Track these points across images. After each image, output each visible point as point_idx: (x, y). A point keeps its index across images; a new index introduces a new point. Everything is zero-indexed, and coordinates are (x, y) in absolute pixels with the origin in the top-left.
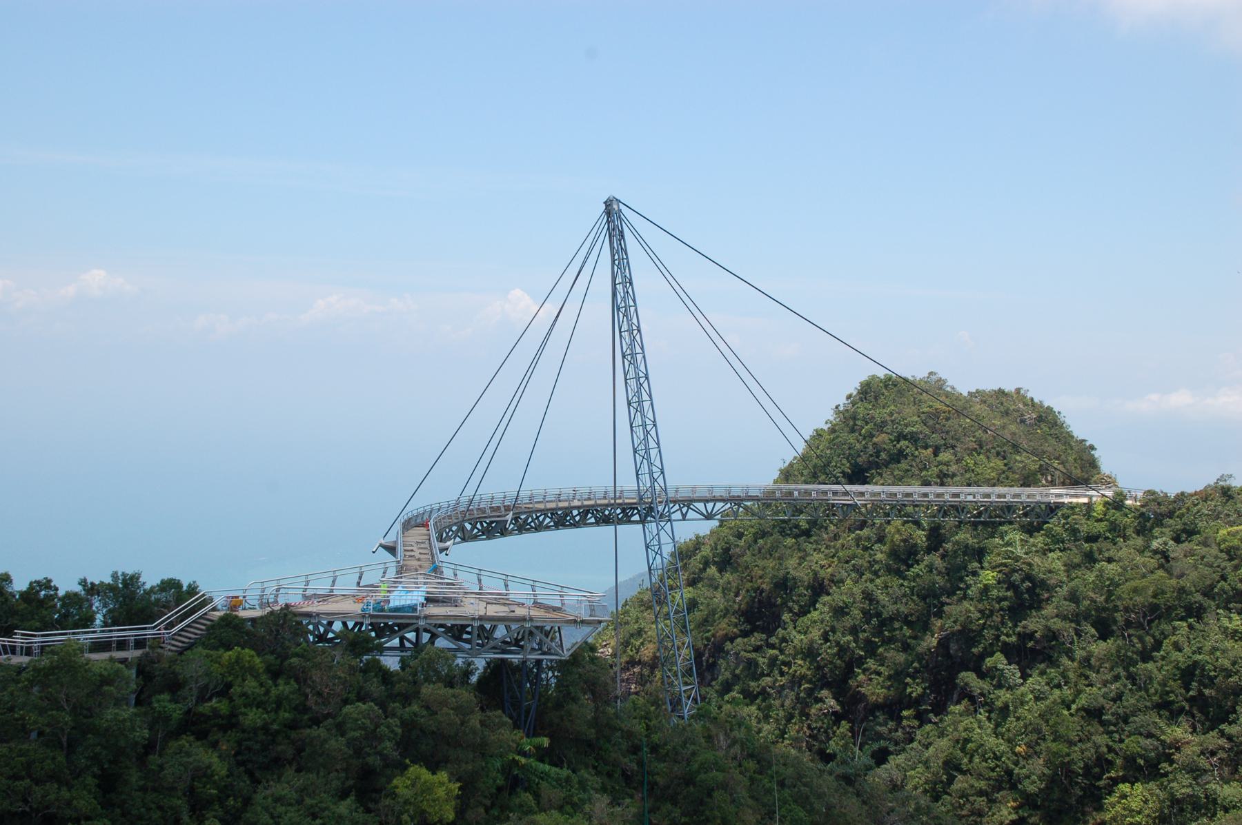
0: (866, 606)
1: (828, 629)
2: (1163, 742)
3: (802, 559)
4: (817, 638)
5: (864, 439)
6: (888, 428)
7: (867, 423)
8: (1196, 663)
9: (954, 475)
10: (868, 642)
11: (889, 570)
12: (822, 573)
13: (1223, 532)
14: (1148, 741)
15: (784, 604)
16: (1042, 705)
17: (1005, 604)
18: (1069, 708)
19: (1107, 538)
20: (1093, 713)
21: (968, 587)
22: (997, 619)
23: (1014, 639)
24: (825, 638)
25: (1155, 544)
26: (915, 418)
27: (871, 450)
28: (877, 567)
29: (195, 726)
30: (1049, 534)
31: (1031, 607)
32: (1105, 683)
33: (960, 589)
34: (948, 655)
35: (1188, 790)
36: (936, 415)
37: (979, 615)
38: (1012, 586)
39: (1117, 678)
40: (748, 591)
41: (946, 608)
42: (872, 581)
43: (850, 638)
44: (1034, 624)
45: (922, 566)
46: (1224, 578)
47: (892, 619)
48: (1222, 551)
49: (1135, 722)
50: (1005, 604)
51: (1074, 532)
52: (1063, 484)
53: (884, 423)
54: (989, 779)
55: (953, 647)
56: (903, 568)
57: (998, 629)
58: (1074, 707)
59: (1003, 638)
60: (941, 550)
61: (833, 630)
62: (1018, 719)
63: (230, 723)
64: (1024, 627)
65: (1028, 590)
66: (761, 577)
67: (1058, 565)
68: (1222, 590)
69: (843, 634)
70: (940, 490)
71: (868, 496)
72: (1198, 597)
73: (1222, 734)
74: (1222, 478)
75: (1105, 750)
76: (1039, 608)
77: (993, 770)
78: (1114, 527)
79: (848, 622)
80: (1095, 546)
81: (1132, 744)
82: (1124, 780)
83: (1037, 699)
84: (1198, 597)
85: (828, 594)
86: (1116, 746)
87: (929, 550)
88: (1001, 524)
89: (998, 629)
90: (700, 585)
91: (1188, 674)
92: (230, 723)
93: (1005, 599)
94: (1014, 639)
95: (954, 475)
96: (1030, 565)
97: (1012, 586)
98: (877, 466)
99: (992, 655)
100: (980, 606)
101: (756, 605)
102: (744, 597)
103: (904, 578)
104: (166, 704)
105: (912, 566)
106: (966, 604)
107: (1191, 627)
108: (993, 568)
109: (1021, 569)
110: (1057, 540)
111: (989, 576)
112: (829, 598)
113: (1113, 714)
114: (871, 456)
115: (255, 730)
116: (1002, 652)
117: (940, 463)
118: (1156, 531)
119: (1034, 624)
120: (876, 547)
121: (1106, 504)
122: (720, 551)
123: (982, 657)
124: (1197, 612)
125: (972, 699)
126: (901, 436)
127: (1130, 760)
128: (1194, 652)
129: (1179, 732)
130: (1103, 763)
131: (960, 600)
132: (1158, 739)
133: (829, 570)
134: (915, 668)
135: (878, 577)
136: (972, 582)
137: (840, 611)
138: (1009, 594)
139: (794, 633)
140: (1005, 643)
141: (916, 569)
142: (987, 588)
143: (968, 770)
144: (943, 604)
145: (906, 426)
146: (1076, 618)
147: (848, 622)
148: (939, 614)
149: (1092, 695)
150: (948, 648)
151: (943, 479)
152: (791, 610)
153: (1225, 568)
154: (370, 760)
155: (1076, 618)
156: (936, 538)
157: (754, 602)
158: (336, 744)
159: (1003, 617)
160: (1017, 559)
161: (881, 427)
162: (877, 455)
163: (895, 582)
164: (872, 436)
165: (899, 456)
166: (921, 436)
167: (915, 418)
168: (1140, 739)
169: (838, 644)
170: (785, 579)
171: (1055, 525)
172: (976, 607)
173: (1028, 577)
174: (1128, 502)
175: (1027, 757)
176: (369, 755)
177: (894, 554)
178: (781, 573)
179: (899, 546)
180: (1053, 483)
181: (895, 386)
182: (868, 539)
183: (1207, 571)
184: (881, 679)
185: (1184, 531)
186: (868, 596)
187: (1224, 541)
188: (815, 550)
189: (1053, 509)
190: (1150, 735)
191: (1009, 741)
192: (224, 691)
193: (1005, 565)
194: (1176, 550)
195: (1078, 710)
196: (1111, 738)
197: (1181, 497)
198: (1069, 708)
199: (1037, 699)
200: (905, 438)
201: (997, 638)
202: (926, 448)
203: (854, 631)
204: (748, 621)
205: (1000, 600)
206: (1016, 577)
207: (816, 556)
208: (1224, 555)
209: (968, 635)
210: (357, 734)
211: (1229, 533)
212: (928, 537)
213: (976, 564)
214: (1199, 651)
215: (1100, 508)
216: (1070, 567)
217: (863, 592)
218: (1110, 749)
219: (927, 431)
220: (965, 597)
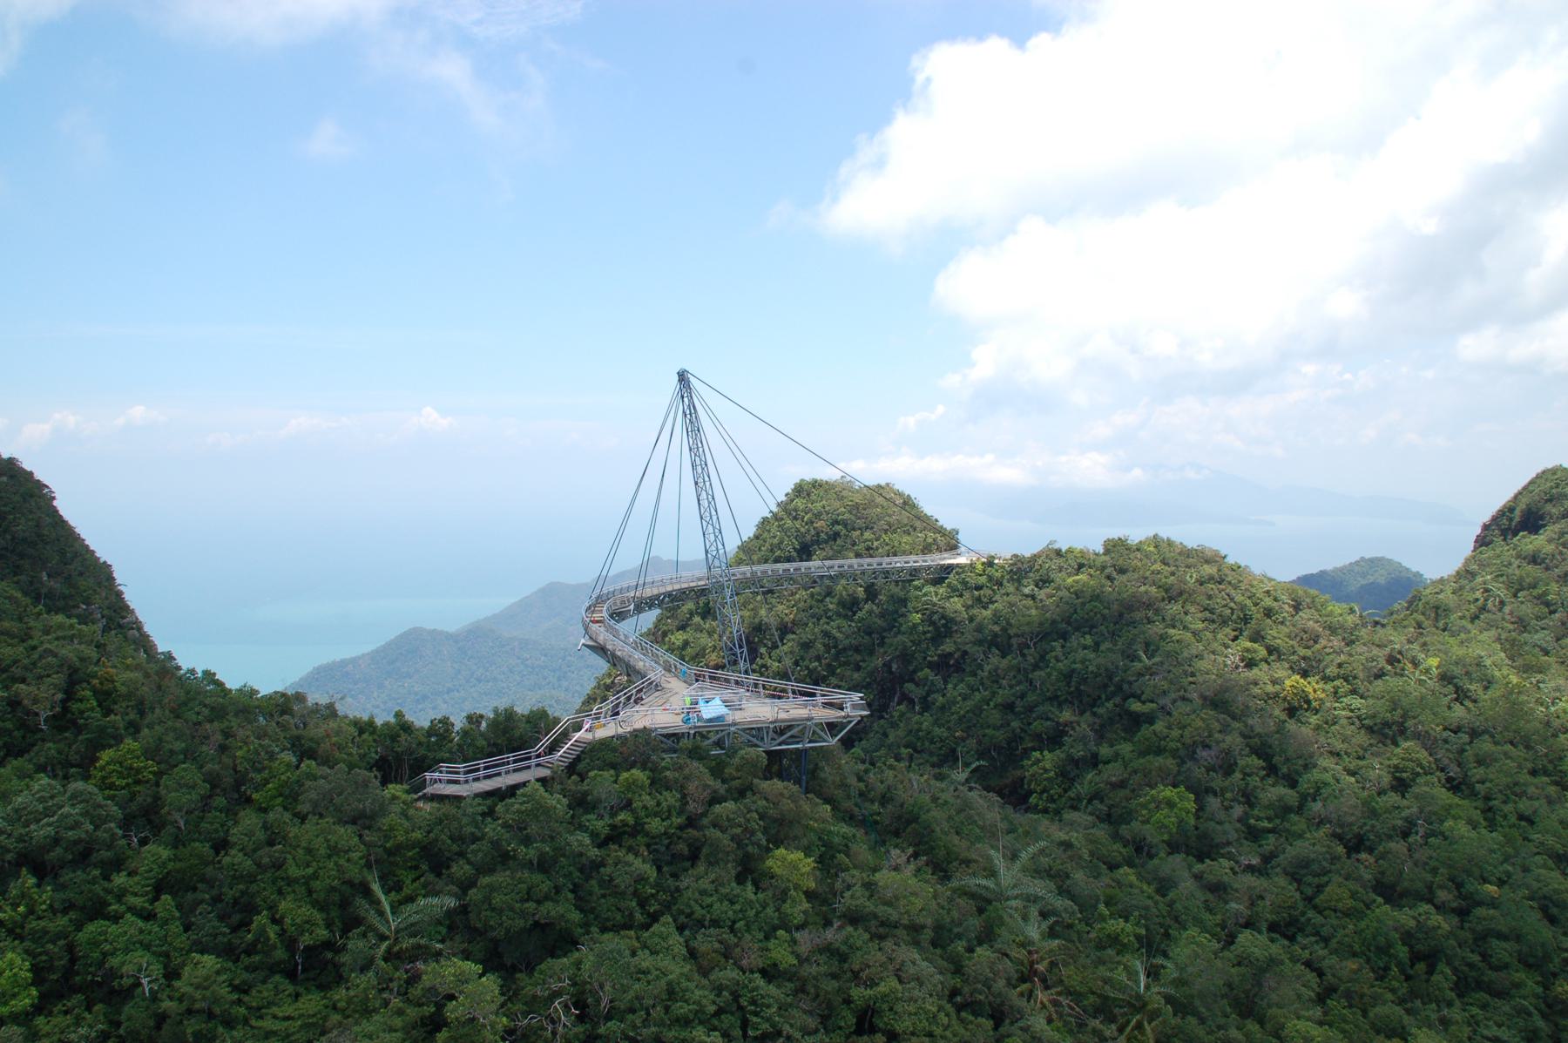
0: (826, 641)
2: (1058, 723)
3: (771, 609)
5: (807, 524)
6: (824, 516)
7: (806, 514)
8: (1073, 671)
9: (877, 549)
10: (829, 665)
11: (839, 615)
12: (786, 619)
13: (1070, 580)
14: (1049, 723)
15: (761, 641)
16: (969, 703)
17: (929, 635)
18: (988, 705)
20: (1009, 707)
22: (924, 646)
23: (936, 658)
24: (796, 663)
25: (1027, 591)
26: (843, 510)
27: (813, 532)
28: (830, 614)
29: (615, 836)
30: (949, 586)
31: (945, 637)
32: (1011, 687)
33: (895, 627)
34: (891, 672)
35: (1082, 753)
36: (857, 506)
37: (911, 644)
38: (932, 623)
39: (1019, 683)
41: (886, 640)
42: (828, 624)
43: (817, 664)
44: (948, 646)
45: (864, 612)
46: (1076, 612)
47: (845, 649)
50: (929, 635)
51: (964, 583)
52: (946, 550)
53: (820, 513)
54: (939, 755)
55: (894, 667)
56: (850, 613)
57: (924, 653)
58: (992, 704)
59: (929, 658)
61: (802, 658)
62: (953, 714)
63: (637, 829)
64: (943, 650)
65: (943, 625)
67: (959, 607)
68: (1076, 620)
69: (810, 660)
70: (869, 560)
71: (836, 568)
73: (1094, 714)
74: (1051, 543)
75: (1019, 730)
76: (951, 637)
77: (940, 749)
78: (990, 578)
79: (813, 653)
80: (982, 592)
81: (1037, 726)
82: (1034, 749)
83: (964, 699)
85: (794, 633)
86: (1026, 728)
87: (866, 601)
88: (913, 580)
89: (924, 653)
90: (688, 629)
91: (1068, 676)
92: (637, 829)
93: (929, 632)
94: (936, 658)
95: (877, 549)
97: (932, 623)
98: (818, 542)
99: (922, 669)
100: (912, 638)
103: (852, 621)
104: (595, 823)
105: (856, 612)
106: (900, 637)
107: (1063, 647)
108: (917, 612)
110: (954, 590)
111: (917, 617)
112: (794, 636)
115: (659, 836)
116: (928, 667)
117: (866, 540)
118: (1025, 582)
119: (948, 646)
120: (828, 599)
121: (983, 564)
122: (701, 605)
123: (915, 672)
124: (1064, 636)
125: (912, 702)
126: (836, 522)
127: (1038, 737)
129: (1066, 715)
130: (1015, 739)
131: (895, 636)
133: (792, 616)
135: (833, 621)
137: (806, 646)
138: (930, 629)
139: (770, 661)
140: (929, 662)
141: (860, 614)
142: (915, 626)
143: (922, 751)
145: (838, 515)
146: (979, 642)
147: (813, 653)
148: (882, 644)
149: (1003, 695)
150: (890, 667)
151: (870, 551)
152: (765, 646)
154: (750, 849)
155: (979, 642)
156: (871, 592)
158: (725, 840)
159: (928, 644)
160: (935, 605)
161: (818, 516)
162: (818, 534)
163: (844, 623)
164: (812, 523)
165: (836, 536)
167: (843, 510)
168: (1042, 721)
169: (807, 668)
170: (760, 624)
171: (952, 579)
173: (943, 617)
174: (996, 561)
175: (963, 739)
176: (747, 845)
177: (842, 603)
178: (757, 620)
180: (939, 550)
182: (819, 594)
185: (1041, 580)
186: (826, 634)
187: (1072, 587)
189: (949, 569)
190: (1048, 719)
191: (949, 728)
192: (628, 805)
193: (926, 609)
194: (1041, 594)
195: (995, 707)
197: (1034, 558)
198: (988, 705)
199: (964, 699)
201: (925, 658)
202: (854, 529)
205: (925, 633)
206: (935, 617)
207: (781, 607)
208: (1073, 596)
209: (905, 657)
210: (738, 830)
212: (865, 591)
213: (904, 609)
214: (1074, 662)
215: (980, 567)
216: (968, 608)
219: (853, 518)
220: (899, 632)
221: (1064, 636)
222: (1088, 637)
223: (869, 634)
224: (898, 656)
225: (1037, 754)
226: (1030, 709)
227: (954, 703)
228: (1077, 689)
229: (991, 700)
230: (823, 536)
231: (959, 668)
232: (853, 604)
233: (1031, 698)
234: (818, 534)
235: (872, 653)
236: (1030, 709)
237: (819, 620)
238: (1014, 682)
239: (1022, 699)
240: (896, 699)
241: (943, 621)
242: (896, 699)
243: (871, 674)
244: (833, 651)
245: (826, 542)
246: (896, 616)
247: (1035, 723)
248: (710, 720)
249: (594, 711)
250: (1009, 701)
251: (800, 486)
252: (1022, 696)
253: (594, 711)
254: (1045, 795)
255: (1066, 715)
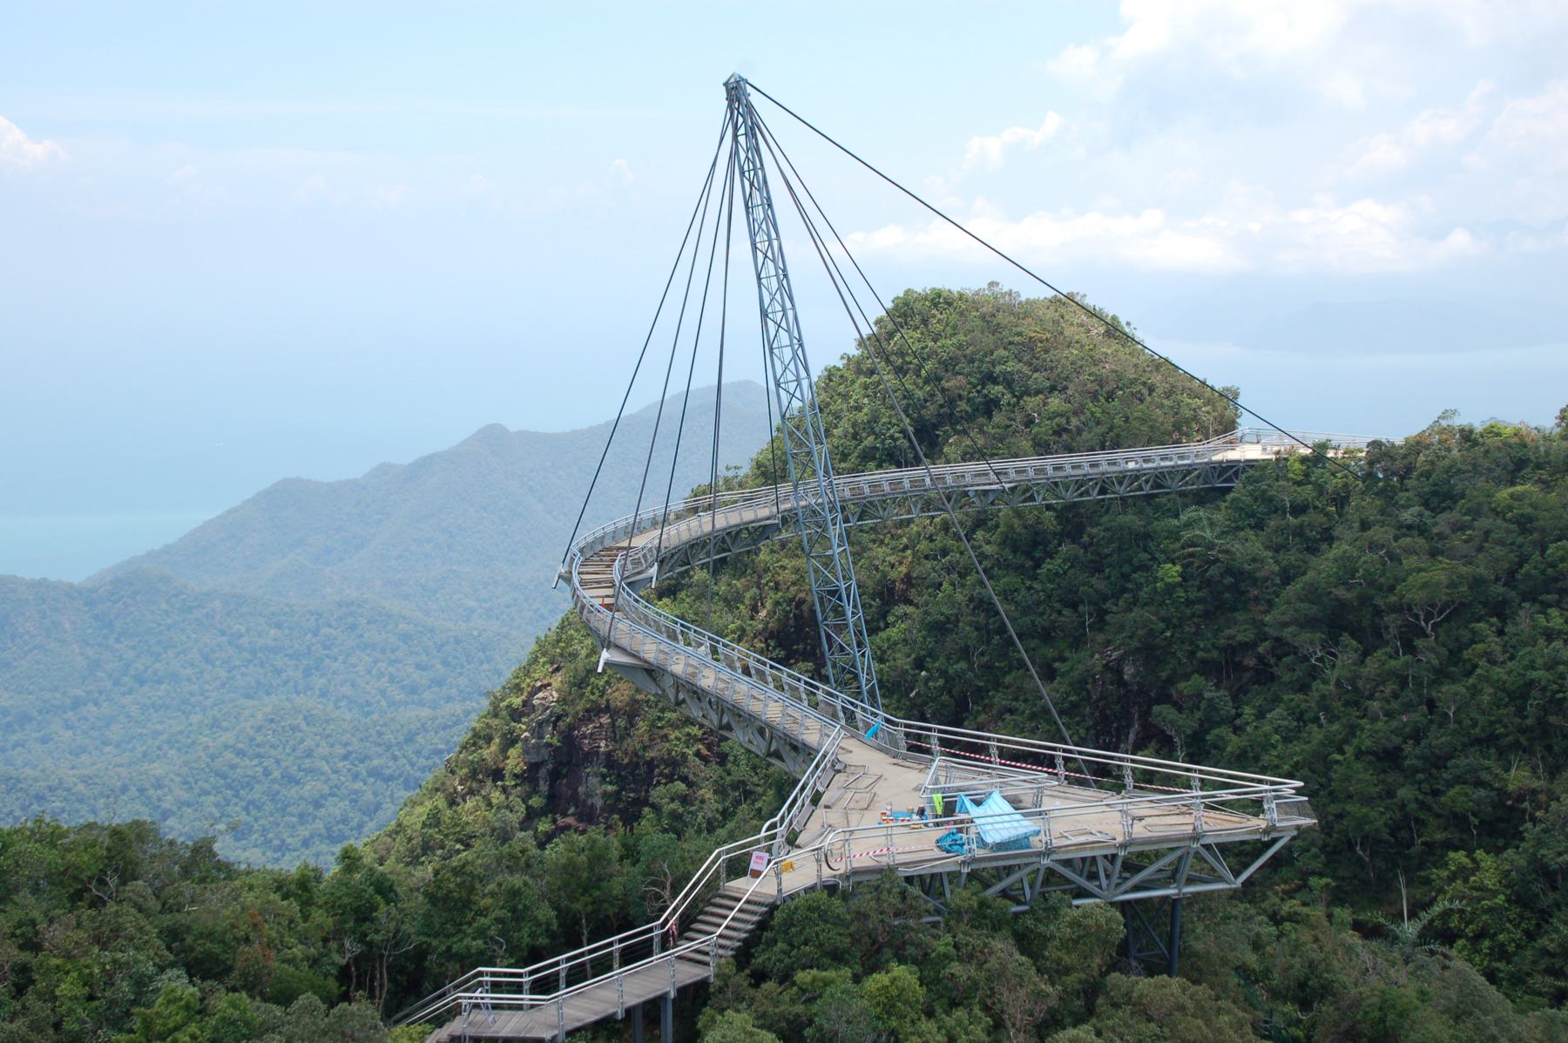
0: (981, 618)
1: (923, 653)
2: (1501, 792)
4: (907, 667)
6: (963, 366)
8: (1531, 684)
9: (1079, 431)
10: (988, 667)
12: (893, 575)
14: (1482, 792)
18: (1342, 752)
19: (1315, 508)
20: (1389, 758)
21: (1139, 586)
22: (1189, 629)
23: (1215, 654)
24: (919, 664)
25: (1407, 516)
26: (1002, 352)
27: (940, 399)
32: (1389, 715)
34: (1121, 682)
37: (1162, 625)
39: (1408, 707)
40: (777, 603)
43: (963, 665)
48: (1510, 521)
49: (1457, 767)
50: (1199, 608)
52: (1217, 433)
55: (1128, 671)
56: (1029, 563)
58: (1349, 749)
60: (1085, 538)
66: (794, 584)
72: (1499, 589)
74: (1445, 415)
75: (1413, 806)
79: (952, 642)
80: (1304, 518)
81: (1456, 797)
83: (1286, 740)
84: (1499, 589)
85: (909, 602)
86: (1429, 800)
90: (682, 595)
91: (1519, 695)
95: (1079, 431)
96: (1227, 552)
98: (951, 419)
100: (1163, 613)
101: (791, 622)
102: (771, 614)
106: (1137, 613)
109: (1217, 560)
111: (1171, 572)
112: (910, 609)
113: (1417, 757)
114: (941, 406)
123: (1170, 681)
124: (1501, 611)
126: (990, 378)
127: (1458, 820)
128: (1526, 668)
129: (1518, 777)
130: (1404, 824)
132: (1493, 789)
134: (1071, 702)
136: (1143, 580)
137: (939, 628)
140: (1203, 662)
142: (1170, 589)
144: (1106, 612)
146: (1309, 623)
147: (952, 642)
149: (1376, 731)
150: (1119, 672)
153: (1520, 547)
155: (1309, 623)
157: (788, 618)
159: (1198, 626)
160: (1211, 546)
161: (949, 365)
162: (951, 402)
164: (939, 379)
166: (1016, 377)
168: (1468, 789)
172: (1156, 614)
173: (1229, 571)
174: (1330, 454)
179: (1020, 534)
181: (950, 304)
183: (1499, 551)
184: (1019, 718)
185: (1435, 493)
186: (983, 605)
187: (1511, 508)
188: (874, 541)
190: (1479, 783)
193: (1192, 555)
196: (1420, 789)
198: (1342, 752)
199: (1286, 740)
200: (995, 381)
201: (1192, 654)
202: (1027, 393)
203: (965, 653)
204: (780, 645)
205: (1189, 603)
207: (880, 551)
208: (1513, 527)
211: (1512, 496)
213: (1144, 556)
214: (1532, 666)
217: (971, 600)
218: (1423, 805)
219: (1025, 369)
221: (1501, 611)
222: (1553, 612)
223: (1074, 606)
224: (1137, 650)
225: (1459, 857)
226: (1438, 762)
227: (1267, 746)
228: (1542, 722)
229: (1346, 741)
230: (963, 406)
231: (1264, 675)
232: (1035, 544)
233: (1439, 739)
234: (951, 402)
235: (1078, 642)
236: (1438, 762)
237: (962, 576)
238: (1395, 705)
239: (1418, 742)
240: (1132, 737)
241: (1228, 580)
242: (1132, 737)
243: (1080, 684)
244: (996, 639)
245: (970, 418)
246: (1126, 569)
247: (1451, 793)
248: (1000, 846)
249: (763, 834)
250: (1390, 746)
251: (906, 304)
252: (1417, 735)
253: (763, 834)
254: (1487, 943)
255: (1518, 777)
